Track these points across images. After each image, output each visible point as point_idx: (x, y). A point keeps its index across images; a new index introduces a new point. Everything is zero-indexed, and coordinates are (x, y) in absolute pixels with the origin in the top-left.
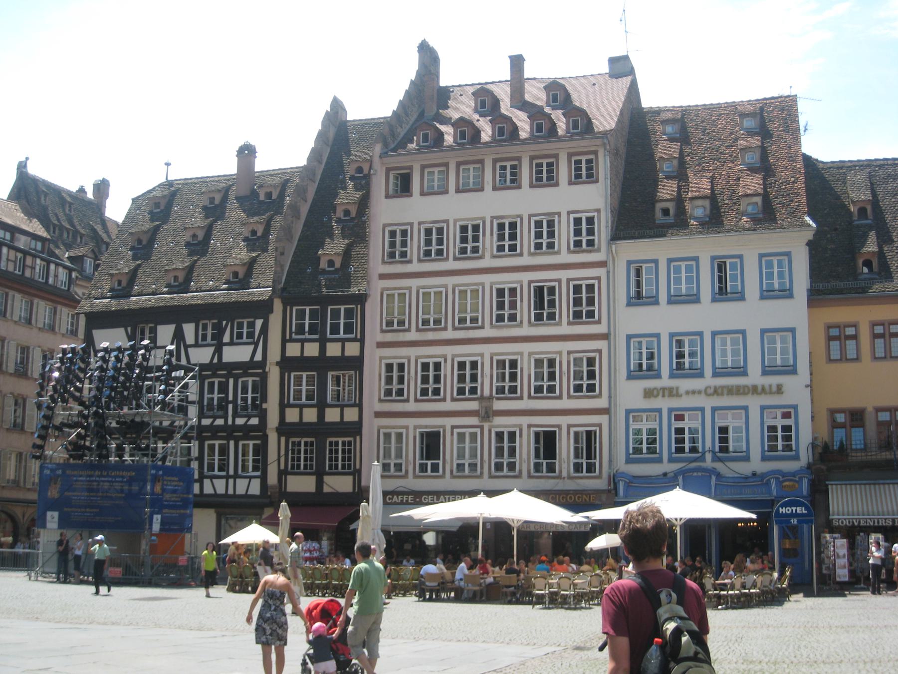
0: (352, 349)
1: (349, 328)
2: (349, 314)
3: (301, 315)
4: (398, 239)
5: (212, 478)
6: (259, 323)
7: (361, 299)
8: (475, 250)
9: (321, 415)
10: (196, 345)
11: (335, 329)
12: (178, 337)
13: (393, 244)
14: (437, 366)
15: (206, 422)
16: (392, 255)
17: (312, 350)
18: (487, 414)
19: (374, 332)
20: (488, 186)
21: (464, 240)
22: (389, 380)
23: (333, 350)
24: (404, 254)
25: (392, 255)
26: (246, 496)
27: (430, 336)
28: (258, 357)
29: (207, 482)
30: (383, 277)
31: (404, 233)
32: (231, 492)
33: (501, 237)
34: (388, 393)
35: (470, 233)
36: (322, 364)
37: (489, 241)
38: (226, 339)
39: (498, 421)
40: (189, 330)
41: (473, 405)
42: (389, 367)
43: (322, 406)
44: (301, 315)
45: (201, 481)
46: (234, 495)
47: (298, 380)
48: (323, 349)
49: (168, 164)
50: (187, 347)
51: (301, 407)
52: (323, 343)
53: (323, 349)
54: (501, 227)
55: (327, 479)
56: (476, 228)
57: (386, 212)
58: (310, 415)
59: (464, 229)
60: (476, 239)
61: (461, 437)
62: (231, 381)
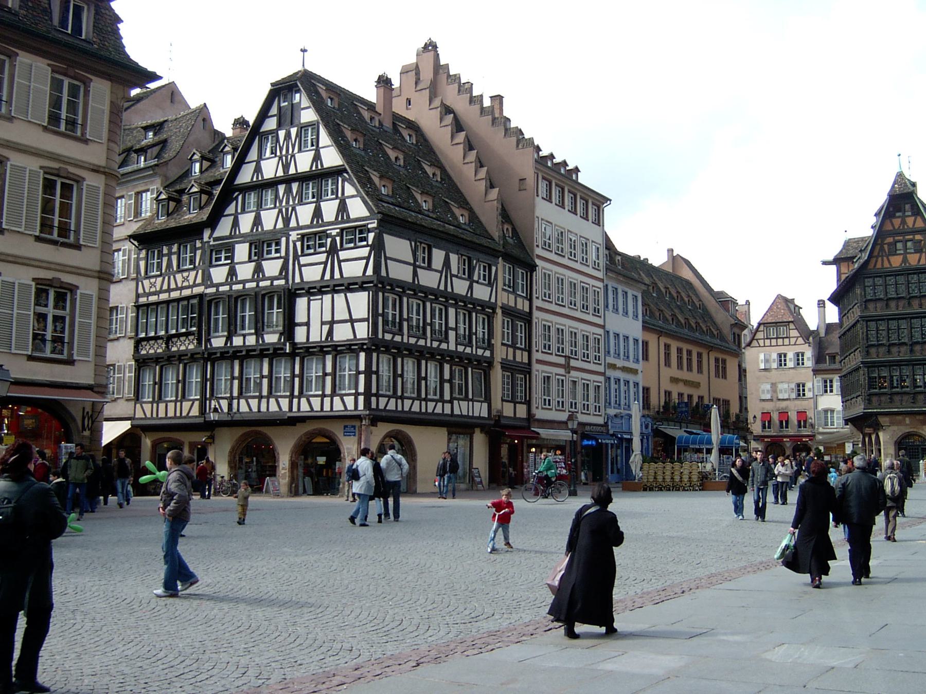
5: (459, 400)
6: (494, 269)
10: (456, 276)
12: (447, 263)
15: (461, 348)
18: (568, 368)
26: (480, 417)
28: (493, 300)
29: (456, 402)
32: (471, 414)
38: (476, 278)
39: (574, 373)
40: (454, 258)
41: (562, 361)
45: (451, 402)
46: (473, 417)
49: (304, 51)
50: (452, 276)
62: (474, 314)
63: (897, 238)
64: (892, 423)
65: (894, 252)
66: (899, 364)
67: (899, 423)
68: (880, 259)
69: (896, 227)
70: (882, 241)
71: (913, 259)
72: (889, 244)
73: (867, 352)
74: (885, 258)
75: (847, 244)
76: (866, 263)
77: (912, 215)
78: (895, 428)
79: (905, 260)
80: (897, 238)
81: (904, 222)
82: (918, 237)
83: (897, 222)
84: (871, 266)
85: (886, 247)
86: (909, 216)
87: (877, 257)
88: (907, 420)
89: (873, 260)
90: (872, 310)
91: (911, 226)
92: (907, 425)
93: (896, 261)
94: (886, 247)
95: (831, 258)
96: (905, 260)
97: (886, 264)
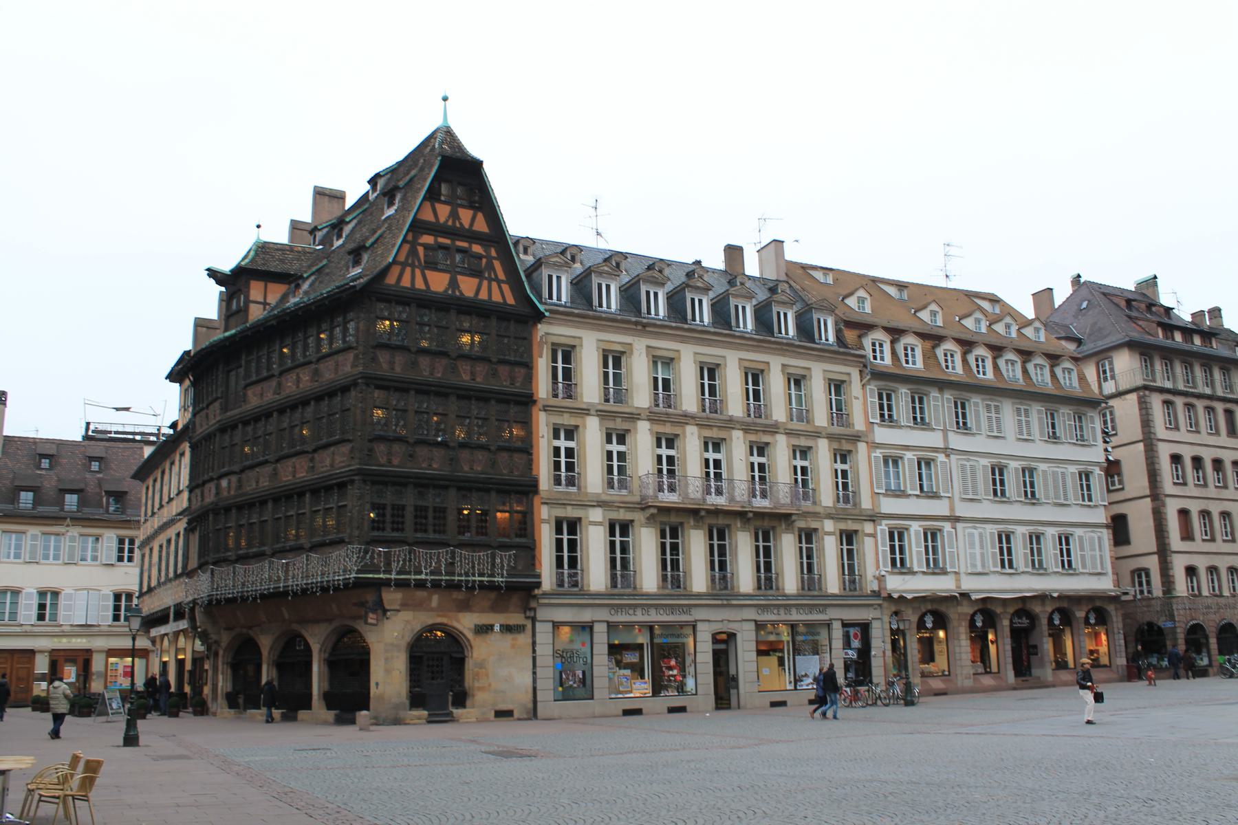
63: (441, 240)
64: (405, 606)
65: (431, 265)
66: (423, 484)
67: (417, 606)
68: (408, 270)
69: (442, 220)
70: (415, 238)
71: (468, 287)
72: (427, 247)
73: (371, 450)
74: (418, 272)
75: (263, 249)
76: (389, 267)
77: (471, 207)
78: (406, 615)
79: (453, 284)
80: (441, 240)
81: (454, 215)
82: (477, 249)
83: (444, 211)
84: (391, 279)
85: (421, 250)
86: (463, 206)
87: (404, 265)
88: (435, 600)
89: (396, 270)
90: (385, 366)
91: (467, 227)
92: (432, 610)
93: (438, 282)
94: (421, 250)
95: (226, 266)
96: (453, 284)
97: (420, 284)
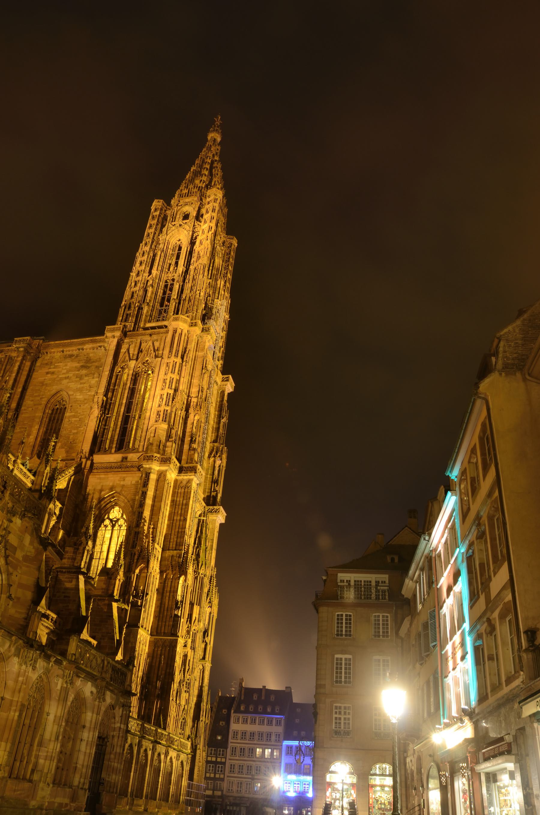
0: (223, 760)
1: (223, 755)
2: (223, 751)
3: (212, 750)
4: (236, 733)
7: (226, 748)
8: (253, 739)
9: (215, 776)
11: (220, 755)
13: (234, 735)
14: (243, 766)
16: (234, 737)
17: (214, 759)
19: (228, 757)
20: (257, 724)
21: (251, 736)
22: (231, 768)
23: (219, 760)
24: (237, 738)
25: (234, 737)
27: (241, 758)
30: (231, 742)
31: (237, 732)
33: (259, 736)
34: (231, 771)
35: (252, 734)
36: (216, 763)
37: (256, 737)
42: (231, 765)
43: (215, 773)
44: (212, 750)
47: (210, 766)
48: (216, 759)
51: (210, 773)
52: (217, 758)
53: (216, 759)
54: (259, 734)
55: (215, 792)
56: (253, 733)
57: (234, 727)
58: (212, 775)
59: (251, 733)
60: (253, 736)
61: (247, 784)
